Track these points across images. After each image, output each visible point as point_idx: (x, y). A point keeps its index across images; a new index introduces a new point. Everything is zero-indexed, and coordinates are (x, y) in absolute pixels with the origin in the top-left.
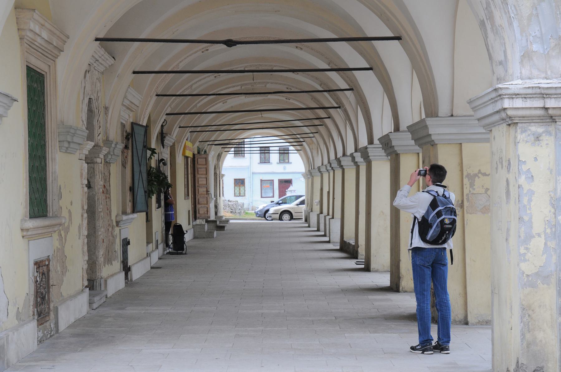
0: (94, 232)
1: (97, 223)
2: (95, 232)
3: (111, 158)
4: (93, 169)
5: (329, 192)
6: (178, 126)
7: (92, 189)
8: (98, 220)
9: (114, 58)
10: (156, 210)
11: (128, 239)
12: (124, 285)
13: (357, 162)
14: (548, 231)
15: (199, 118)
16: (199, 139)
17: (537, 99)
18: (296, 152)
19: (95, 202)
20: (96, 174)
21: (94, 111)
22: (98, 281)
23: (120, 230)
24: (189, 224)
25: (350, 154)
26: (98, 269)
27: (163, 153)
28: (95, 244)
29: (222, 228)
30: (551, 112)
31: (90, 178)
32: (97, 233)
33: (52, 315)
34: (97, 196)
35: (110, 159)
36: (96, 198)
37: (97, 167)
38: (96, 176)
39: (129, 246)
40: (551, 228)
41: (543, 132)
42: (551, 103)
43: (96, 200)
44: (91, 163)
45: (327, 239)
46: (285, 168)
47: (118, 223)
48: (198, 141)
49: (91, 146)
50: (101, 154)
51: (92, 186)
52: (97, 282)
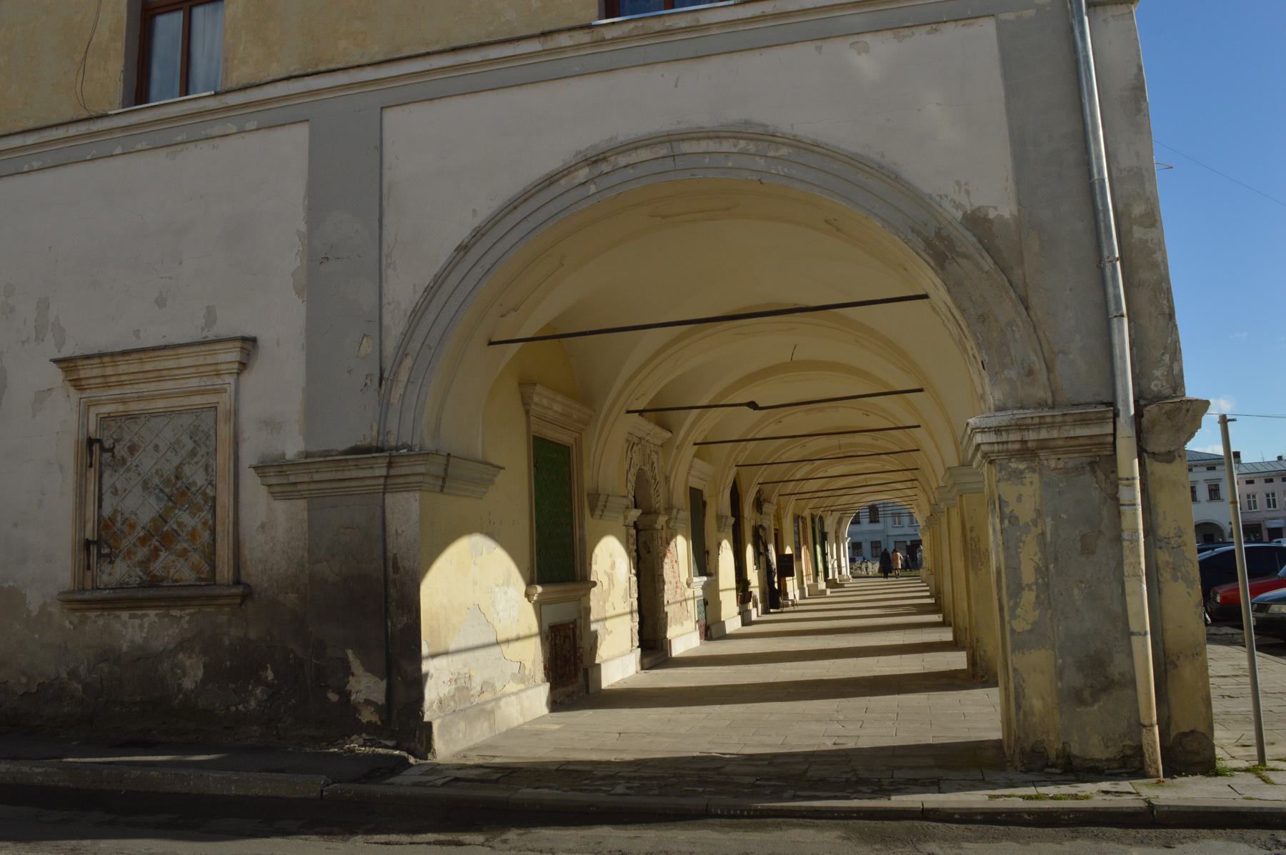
9: (671, 431)
14: (1040, 581)
17: (1013, 432)
29: (841, 586)
30: (1030, 445)
33: (581, 675)
40: (1043, 579)
41: (1027, 468)
42: (1031, 435)
47: (689, 585)
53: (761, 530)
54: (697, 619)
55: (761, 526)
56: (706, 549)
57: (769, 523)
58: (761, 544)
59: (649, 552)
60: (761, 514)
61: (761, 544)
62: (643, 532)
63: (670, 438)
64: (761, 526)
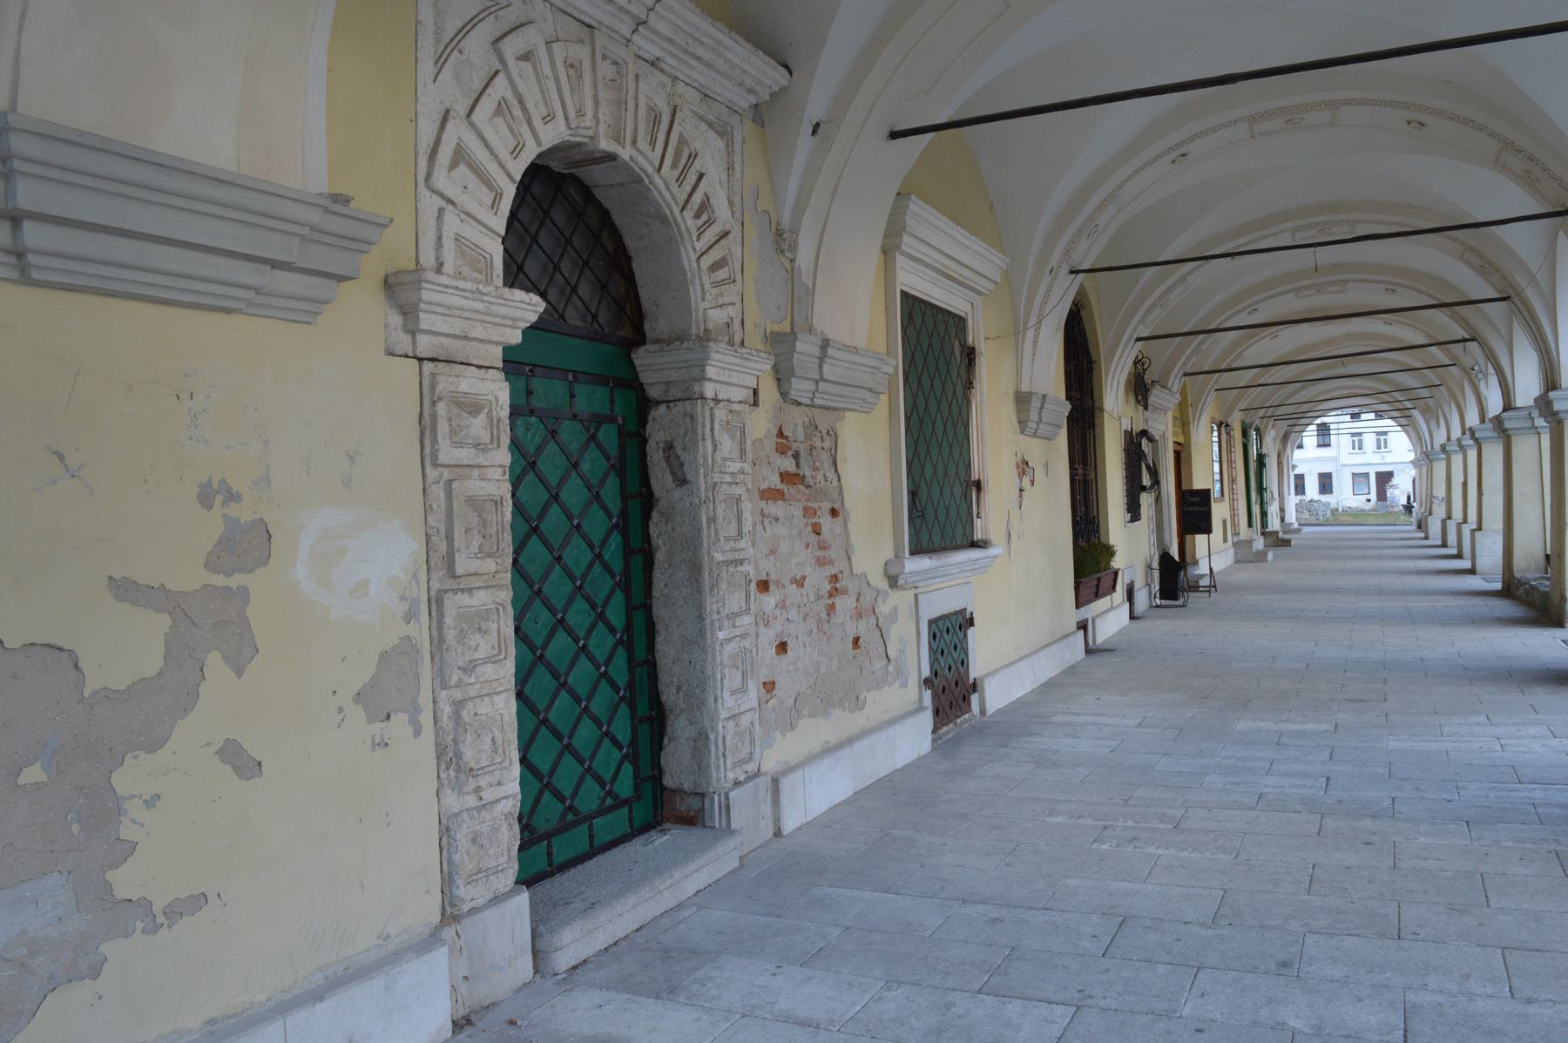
0: (700, 631)
1: (708, 603)
2: (702, 632)
3: (817, 390)
4: (692, 418)
5: (1465, 484)
6: (1181, 373)
7: (688, 486)
8: (712, 590)
9: (786, 67)
10: (1125, 526)
11: (969, 611)
12: (931, 748)
13: (1557, 413)
15: (1201, 343)
16: (1239, 405)
18: (1399, 429)
19: (699, 530)
20: (700, 437)
21: (675, 221)
22: (719, 796)
23: (916, 596)
24: (1225, 540)
25: (1535, 400)
26: (718, 758)
27: (1149, 422)
28: (702, 672)
29: (1287, 543)
31: (684, 450)
32: (708, 635)
34: (707, 511)
35: (814, 394)
36: (704, 518)
37: (703, 413)
38: (700, 443)
39: (971, 628)
43: (704, 523)
44: (684, 400)
45: (1465, 564)
46: (1383, 458)
47: (893, 581)
48: (1238, 409)
49: (536, 312)
50: (710, 365)
51: (688, 477)
52: (713, 800)
53: (1144, 442)
54: (926, 672)
55: (1144, 433)
56: (975, 477)
57: (1163, 426)
58: (1144, 467)
59: (682, 481)
60: (1146, 408)
61: (1144, 467)
62: (662, 408)
63: (784, 89)
64: (1144, 433)
